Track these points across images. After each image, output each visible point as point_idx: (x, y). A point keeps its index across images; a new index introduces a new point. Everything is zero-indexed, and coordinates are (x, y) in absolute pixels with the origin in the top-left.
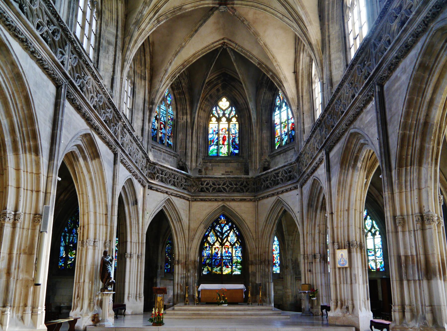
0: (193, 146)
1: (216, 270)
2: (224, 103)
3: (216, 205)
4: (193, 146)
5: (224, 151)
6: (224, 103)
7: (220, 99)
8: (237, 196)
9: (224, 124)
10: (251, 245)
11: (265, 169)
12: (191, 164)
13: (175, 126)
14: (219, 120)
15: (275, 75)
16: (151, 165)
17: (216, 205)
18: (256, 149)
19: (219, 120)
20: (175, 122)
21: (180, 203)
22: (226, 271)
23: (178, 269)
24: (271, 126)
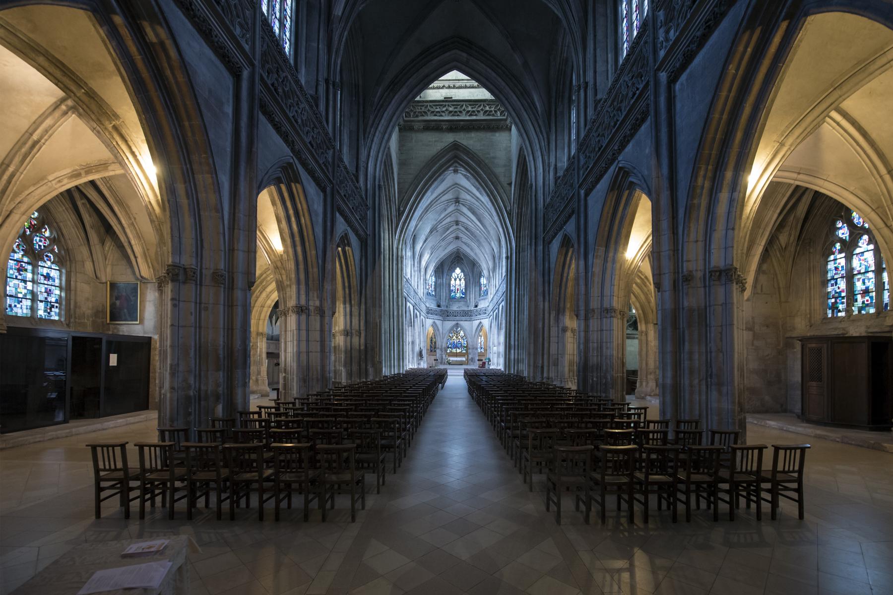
0: (444, 294)
1: (454, 351)
2: (458, 271)
3: (454, 323)
4: (444, 294)
5: (458, 295)
6: (458, 271)
7: (455, 269)
8: (463, 318)
9: (458, 282)
10: (470, 340)
11: (476, 306)
12: (443, 303)
13: (435, 285)
14: (455, 280)
15: (480, 266)
16: (427, 308)
17: (454, 323)
18: (472, 296)
19: (455, 280)
20: (436, 283)
21: (438, 323)
22: (458, 351)
23: (438, 351)
24: (480, 285)
